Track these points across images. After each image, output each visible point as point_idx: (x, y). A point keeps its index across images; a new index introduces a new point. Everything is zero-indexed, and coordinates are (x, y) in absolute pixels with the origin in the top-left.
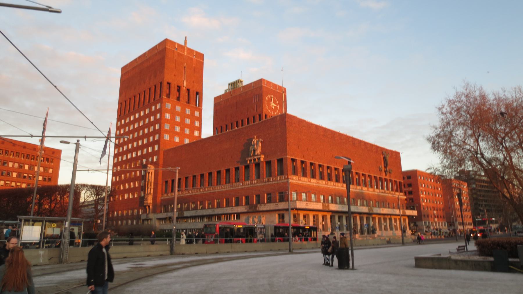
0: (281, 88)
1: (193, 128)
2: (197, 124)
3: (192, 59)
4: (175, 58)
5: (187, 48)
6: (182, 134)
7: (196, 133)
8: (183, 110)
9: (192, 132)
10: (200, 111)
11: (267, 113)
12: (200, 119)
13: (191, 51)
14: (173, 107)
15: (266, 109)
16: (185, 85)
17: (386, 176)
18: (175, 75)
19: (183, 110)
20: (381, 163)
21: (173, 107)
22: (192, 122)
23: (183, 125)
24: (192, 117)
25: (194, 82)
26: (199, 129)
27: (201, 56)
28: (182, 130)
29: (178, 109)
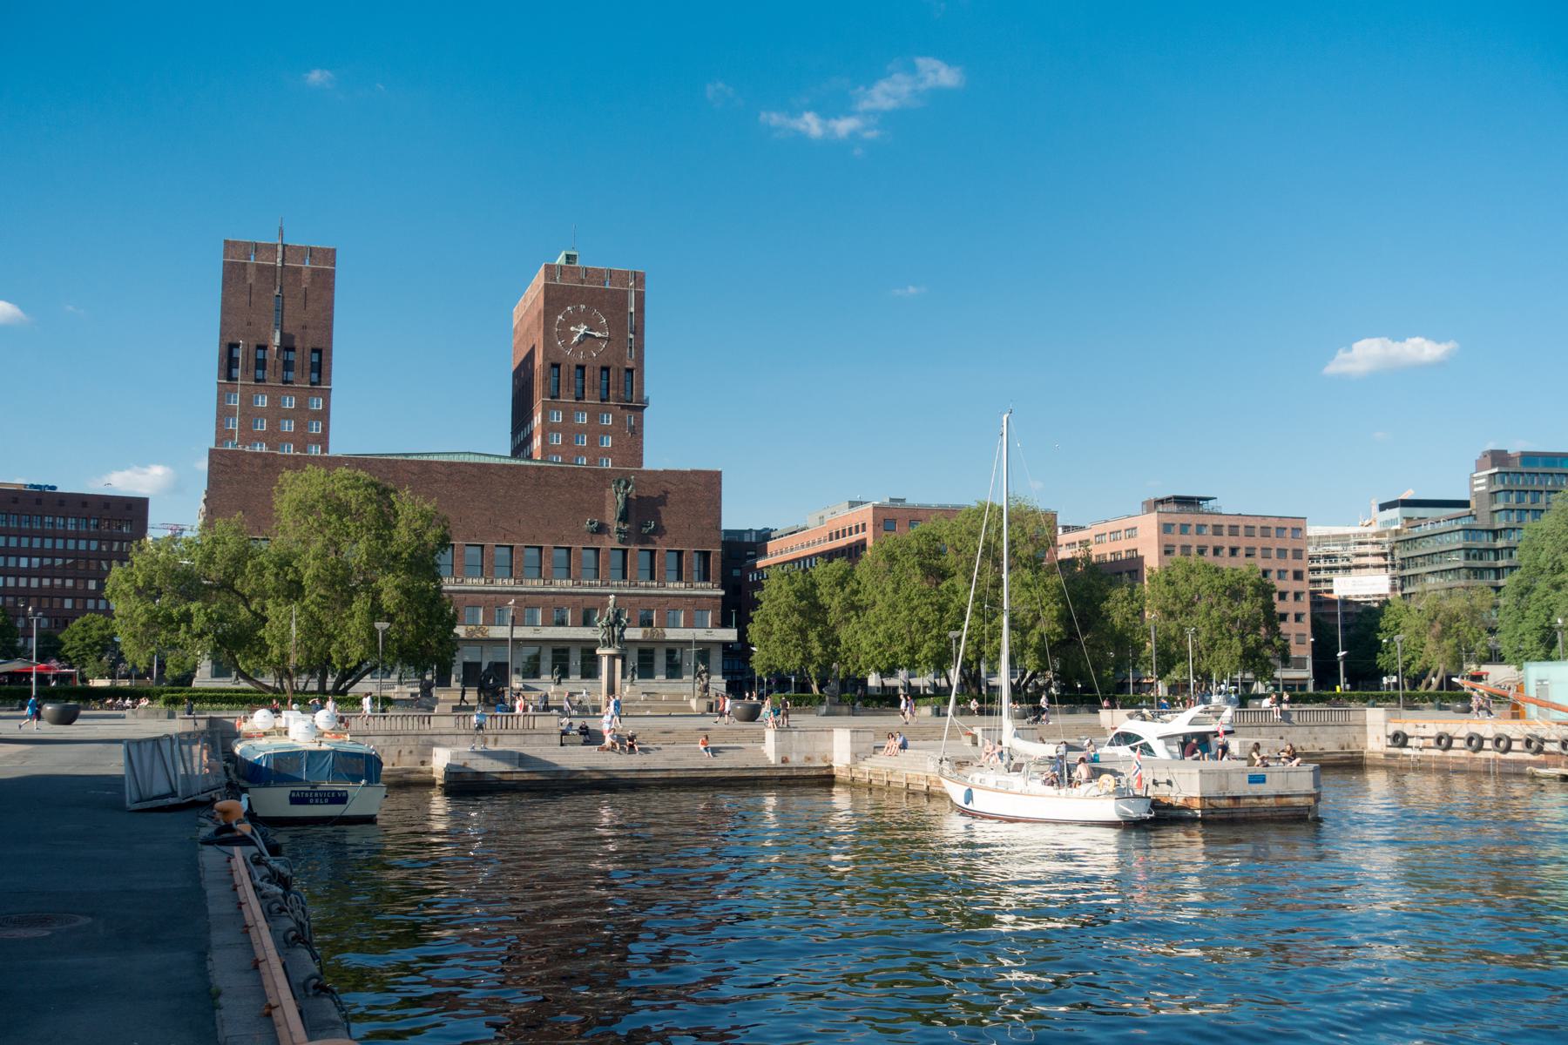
0: (622, 276)
1: (302, 440)
2: (316, 428)
3: (298, 271)
4: (250, 281)
5: (284, 246)
10: (326, 395)
11: (556, 361)
12: (324, 416)
15: (558, 352)
16: (277, 341)
17: (622, 542)
18: (249, 324)
19: (275, 403)
24: (302, 414)
25: (304, 327)
26: (323, 440)
27: (329, 255)
29: (263, 402)
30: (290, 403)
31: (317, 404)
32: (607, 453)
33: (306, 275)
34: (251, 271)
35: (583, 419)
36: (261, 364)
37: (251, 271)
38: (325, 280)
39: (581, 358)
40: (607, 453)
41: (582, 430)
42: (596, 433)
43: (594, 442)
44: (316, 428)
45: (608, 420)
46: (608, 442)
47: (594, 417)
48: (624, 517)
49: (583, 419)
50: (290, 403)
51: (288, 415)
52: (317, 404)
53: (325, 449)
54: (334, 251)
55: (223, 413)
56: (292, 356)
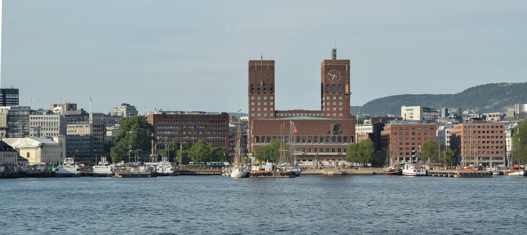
1: (269, 107)
2: (272, 104)
6: (262, 112)
7: (272, 109)
8: (262, 98)
9: (269, 109)
10: (274, 96)
12: (273, 101)
13: (266, 62)
14: (256, 98)
16: (262, 84)
19: (262, 98)
20: (330, 128)
21: (256, 98)
22: (268, 103)
23: (262, 106)
26: (273, 106)
28: (262, 109)
29: (259, 98)
30: (265, 98)
31: (272, 98)
32: (341, 106)
33: (268, 68)
34: (256, 67)
35: (335, 98)
36: (259, 89)
37: (256, 67)
38: (272, 68)
39: (334, 83)
40: (341, 106)
41: (334, 101)
42: (338, 101)
43: (338, 104)
44: (272, 104)
45: (341, 98)
46: (341, 104)
47: (337, 98)
48: (334, 130)
49: (335, 98)
50: (265, 98)
51: (265, 101)
52: (272, 98)
53: (274, 109)
54: (274, 61)
55: (250, 101)
56: (265, 87)
